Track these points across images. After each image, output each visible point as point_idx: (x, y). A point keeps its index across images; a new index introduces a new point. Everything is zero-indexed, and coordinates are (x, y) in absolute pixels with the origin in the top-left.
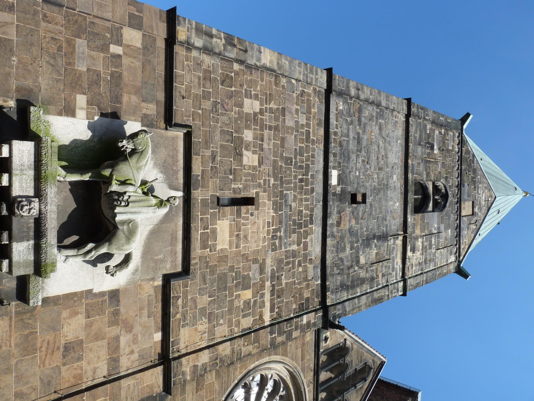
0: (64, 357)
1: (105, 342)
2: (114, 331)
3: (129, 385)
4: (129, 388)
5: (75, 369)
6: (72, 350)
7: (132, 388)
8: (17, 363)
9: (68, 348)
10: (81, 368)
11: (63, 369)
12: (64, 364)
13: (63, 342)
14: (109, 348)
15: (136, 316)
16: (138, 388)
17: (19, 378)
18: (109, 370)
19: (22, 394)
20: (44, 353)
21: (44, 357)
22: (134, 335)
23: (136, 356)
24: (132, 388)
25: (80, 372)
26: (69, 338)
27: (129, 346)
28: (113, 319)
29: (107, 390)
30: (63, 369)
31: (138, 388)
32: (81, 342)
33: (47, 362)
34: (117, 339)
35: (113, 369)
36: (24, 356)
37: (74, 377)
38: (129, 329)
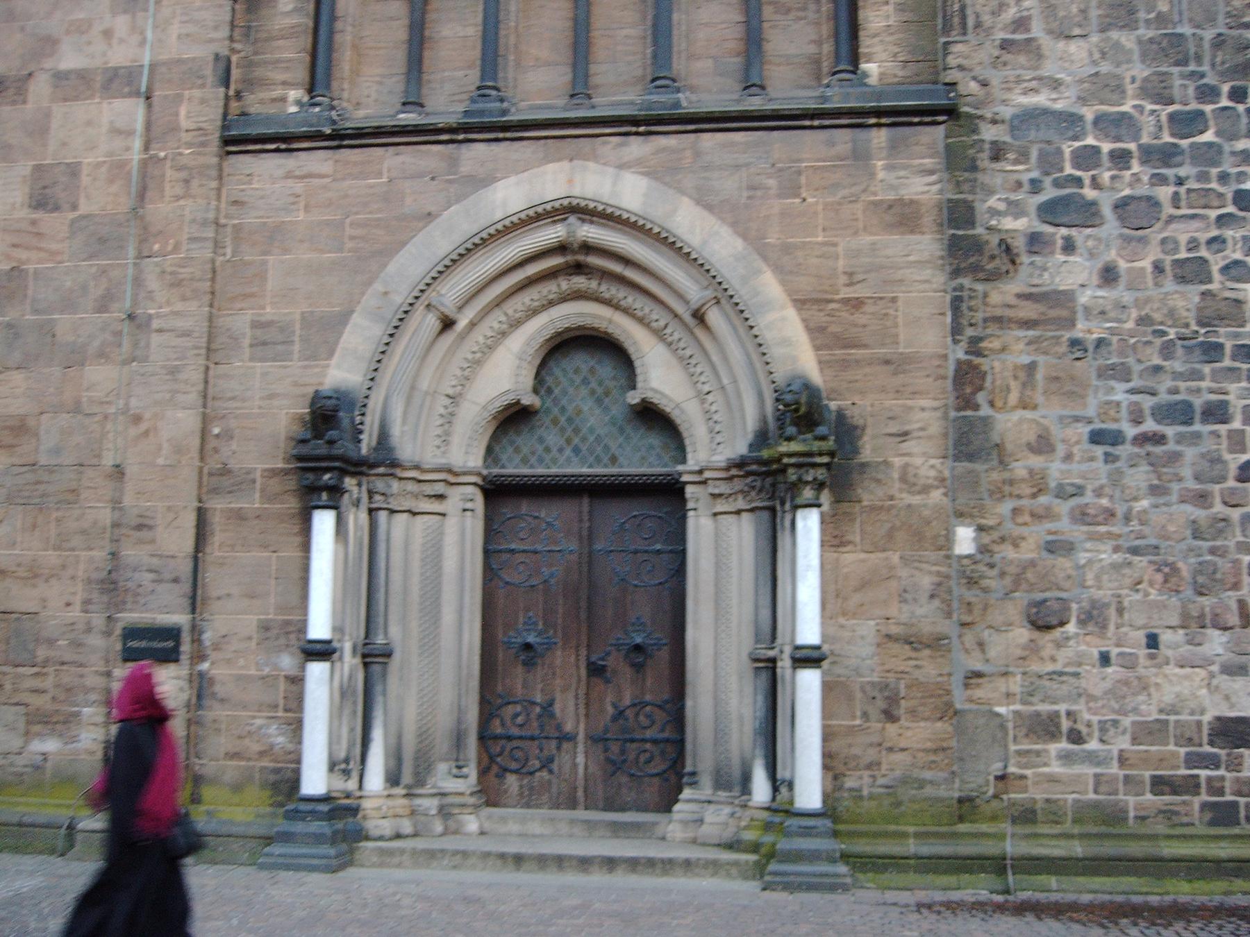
0: (57, 208)
1: (58, 110)
2: (40, 88)
3: (179, 37)
4: (188, 35)
5: (95, 179)
6: (47, 191)
7: (191, 29)
8: (36, 311)
9: (42, 202)
10: (98, 165)
11: (84, 208)
12: (74, 207)
13: (24, 213)
14: (76, 98)
15: (22, 29)
16: (200, 9)
17: (68, 305)
18: (130, 95)
19: (103, 297)
20: (34, 255)
21: (42, 255)
22: (68, 32)
23: (121, 24)
24: (191, 29)
25: (104, 169)
26: (19, 200)
27: (89, 43)
28: (11, 91)
29: (166, 97)
30: (84, 208)
31: (200, 9)
32: (38, 168)
33: (54, 246)
34: (60, 77)
35: (129, 84)
36: (25, 296)
37: (111, 181)
38: (49, 44)
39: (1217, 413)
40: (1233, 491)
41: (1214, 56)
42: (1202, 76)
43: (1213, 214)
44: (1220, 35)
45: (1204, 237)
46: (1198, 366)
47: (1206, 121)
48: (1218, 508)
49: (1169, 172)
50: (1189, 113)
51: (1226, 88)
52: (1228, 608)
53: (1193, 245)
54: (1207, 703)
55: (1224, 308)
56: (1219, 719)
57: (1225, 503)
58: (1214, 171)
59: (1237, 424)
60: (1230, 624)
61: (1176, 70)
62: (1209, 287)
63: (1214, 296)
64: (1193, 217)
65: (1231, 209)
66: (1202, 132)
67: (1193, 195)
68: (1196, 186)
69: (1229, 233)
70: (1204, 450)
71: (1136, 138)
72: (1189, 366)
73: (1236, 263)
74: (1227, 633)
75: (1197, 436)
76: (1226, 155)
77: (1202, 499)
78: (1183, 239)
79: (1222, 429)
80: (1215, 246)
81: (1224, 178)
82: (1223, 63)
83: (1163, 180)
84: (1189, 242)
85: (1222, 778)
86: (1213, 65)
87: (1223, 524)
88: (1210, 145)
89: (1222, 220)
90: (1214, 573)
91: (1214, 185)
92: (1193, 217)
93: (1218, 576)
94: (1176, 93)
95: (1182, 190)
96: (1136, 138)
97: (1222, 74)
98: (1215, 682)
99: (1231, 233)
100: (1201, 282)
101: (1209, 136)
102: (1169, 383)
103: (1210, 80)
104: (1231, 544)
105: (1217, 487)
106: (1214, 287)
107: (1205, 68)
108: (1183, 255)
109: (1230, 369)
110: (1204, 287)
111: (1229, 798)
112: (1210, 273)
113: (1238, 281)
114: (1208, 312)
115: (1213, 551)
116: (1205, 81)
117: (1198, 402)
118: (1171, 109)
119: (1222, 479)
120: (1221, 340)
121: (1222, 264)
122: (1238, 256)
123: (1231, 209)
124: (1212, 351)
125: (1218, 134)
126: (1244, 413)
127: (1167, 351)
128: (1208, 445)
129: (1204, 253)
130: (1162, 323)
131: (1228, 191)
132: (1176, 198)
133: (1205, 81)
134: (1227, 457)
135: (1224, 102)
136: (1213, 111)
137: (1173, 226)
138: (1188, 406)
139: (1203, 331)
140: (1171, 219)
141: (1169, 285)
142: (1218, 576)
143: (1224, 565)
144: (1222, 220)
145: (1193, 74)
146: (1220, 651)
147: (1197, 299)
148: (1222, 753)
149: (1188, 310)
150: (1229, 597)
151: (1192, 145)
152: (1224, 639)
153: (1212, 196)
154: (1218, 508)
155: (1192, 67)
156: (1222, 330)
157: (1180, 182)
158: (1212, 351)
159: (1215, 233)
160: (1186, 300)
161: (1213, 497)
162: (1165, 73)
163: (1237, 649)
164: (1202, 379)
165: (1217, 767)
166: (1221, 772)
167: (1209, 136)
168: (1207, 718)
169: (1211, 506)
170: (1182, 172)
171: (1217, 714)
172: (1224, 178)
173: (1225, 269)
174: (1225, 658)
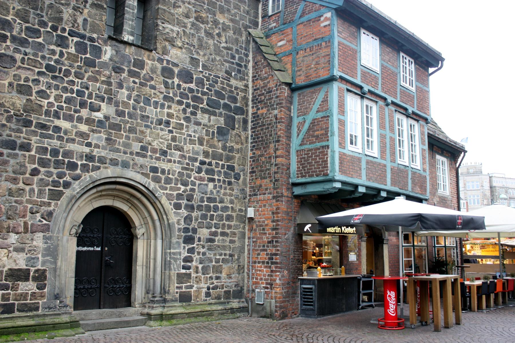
39: (25, 147)
40: (28, 179)
41: (48, 11)
42: (42, 17)
43: (37, 70)
44: (52, 4)
45: (31, 78)
46: (20, 127)
47: (41, 34)
48: (21, 185)
49: (23, 49)
50: (34, 29)
51: (50, 24)
52: (20, 225)
53: (27, 80)
54: (6, 263)
55: (35, 107)
56: (10, 269)
57: (24, 183)
58: (40, 54)
59: (33, 153)
60: (20, 231)
61: (32, 11)
62: (30, 97)
63: (32, 101)
64: (29, 69)
65: (44, 70)
66: (38, 38)
67: (30, 61)
68: (32, 57)
69: (41, 79)
70: (18, 161)
71: (11, 32)
72: (17, 127)
73: (42, 91)
74: (18, 235)
75: (17, 155)
76: (46, 49)
77: (15, 181)
78: (23, 77)
79: (27, 154)
80: (36, 83)
81: (43, 57)
82: (51, 15)
83: (19, 52)
84: (25, 78)
85: (10, 294)
86: (47, 14)
87: (22, 191)
88: (40, 44)
89: (40, 73)
90: (16, 210)
91: (39, 59)
92: (29, 69)
93: (17, 212)
94: (31, 20)
95: (26, 57)
96: (11, 32)
97: (49, 18)
98: (10, 255)
99: (42, 79)
100: (28, 96)
101: (40, 40)
102: (8, 132)
103: (45, 19)
104: (24, 200)
105: (22, 176)
106: (33, 98)
107: (44, 14)
108: (22, 82)
109: (34, 131)
110: (28, 97)
111: (11, 302)
112: (32, 92)
113: (42, 98)
114: (28, 107)
115: (16, 202)
116: (42, 19)
117: (19, 142)
118: (27, 25)
119: (25, 173)
120: (32, 119)
121: (37, 90)
122: (44, 88)
123: (44, 70)
124: (28, 123)
125: (43, 40)
126: (36, 149)
127: (9, 119)
128: (20, 159)
129: (30, 84)
130: (9, 108)
131: (44, 63)
132: (23, 60)
133: (42, 19)
134: (27, 165)
135: (49, 29)
136: (43, 31)
137: (20, 70)
138: (15, 142)
139: (25, 114)
140: (19, 68)
141: (14, 93)
142: (17, 212)
143: (20, 207)
144: (40, 73)
145: (38, 14)
146: (14, 242)
147: (25, 101)
148: (10, 284)
149: (20, 105)
150: (21, 221)
151: (33, 41)
152: (16, 237)
153: (38, 64)
154: (21, 185)
155: (39, 12)
156: (33, 115)
157: (26, 54)
158: (28, 123)
159: (36, 77)
160: (20, 101)
161: (20, 180)
162: (27, 10)
163: (21, 241)
164: (22, 133)
165: (7, 289)
166: (9, 291)
167: (40, 40)
168: (6, 269)
169: (18, 183)
170: (28, 50)
171: (10, 267)
172: (43, 57)
173: (38, 92)
174: (16, 245)
